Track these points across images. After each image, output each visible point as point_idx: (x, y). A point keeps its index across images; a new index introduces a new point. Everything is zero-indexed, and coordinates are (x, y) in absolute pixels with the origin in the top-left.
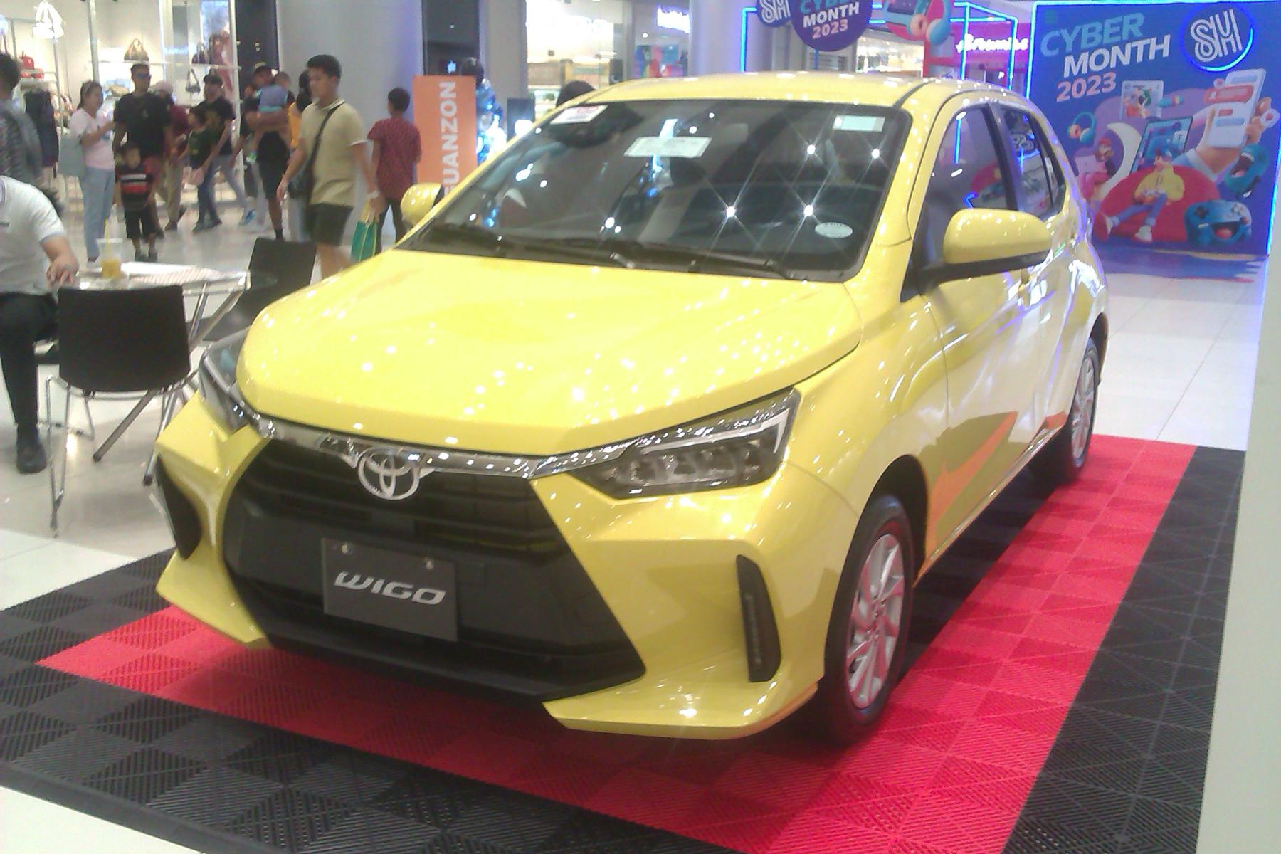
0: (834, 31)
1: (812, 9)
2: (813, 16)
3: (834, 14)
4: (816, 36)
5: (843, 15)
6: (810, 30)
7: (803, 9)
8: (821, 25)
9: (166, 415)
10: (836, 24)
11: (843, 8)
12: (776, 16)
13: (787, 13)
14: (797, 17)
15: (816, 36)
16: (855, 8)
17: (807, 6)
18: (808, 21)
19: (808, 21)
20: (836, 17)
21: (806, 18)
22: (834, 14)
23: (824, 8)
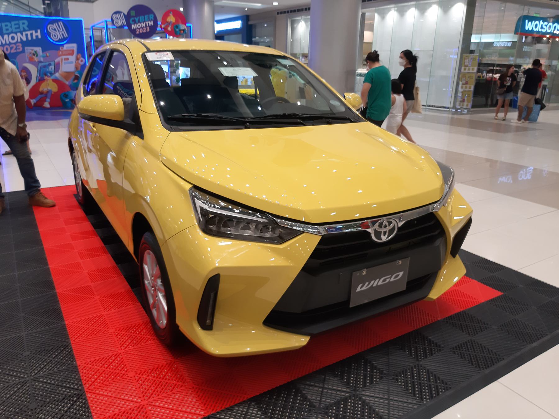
0: (144, 31)
1: (135, 22)
2: (136, 25)
3: (143, 25)
4: (137, 33)
6: (135, 30)
8: (139, 29)
9: (513, 119)
12: (120, 24)
13: (125, 23)
14: (129, 25)
15: (137, 33)
16: (151, 23)
18: (134, 27)
20: (144, 26)
21: (133, 26)
22: (143, 25)
23: (139, 22)
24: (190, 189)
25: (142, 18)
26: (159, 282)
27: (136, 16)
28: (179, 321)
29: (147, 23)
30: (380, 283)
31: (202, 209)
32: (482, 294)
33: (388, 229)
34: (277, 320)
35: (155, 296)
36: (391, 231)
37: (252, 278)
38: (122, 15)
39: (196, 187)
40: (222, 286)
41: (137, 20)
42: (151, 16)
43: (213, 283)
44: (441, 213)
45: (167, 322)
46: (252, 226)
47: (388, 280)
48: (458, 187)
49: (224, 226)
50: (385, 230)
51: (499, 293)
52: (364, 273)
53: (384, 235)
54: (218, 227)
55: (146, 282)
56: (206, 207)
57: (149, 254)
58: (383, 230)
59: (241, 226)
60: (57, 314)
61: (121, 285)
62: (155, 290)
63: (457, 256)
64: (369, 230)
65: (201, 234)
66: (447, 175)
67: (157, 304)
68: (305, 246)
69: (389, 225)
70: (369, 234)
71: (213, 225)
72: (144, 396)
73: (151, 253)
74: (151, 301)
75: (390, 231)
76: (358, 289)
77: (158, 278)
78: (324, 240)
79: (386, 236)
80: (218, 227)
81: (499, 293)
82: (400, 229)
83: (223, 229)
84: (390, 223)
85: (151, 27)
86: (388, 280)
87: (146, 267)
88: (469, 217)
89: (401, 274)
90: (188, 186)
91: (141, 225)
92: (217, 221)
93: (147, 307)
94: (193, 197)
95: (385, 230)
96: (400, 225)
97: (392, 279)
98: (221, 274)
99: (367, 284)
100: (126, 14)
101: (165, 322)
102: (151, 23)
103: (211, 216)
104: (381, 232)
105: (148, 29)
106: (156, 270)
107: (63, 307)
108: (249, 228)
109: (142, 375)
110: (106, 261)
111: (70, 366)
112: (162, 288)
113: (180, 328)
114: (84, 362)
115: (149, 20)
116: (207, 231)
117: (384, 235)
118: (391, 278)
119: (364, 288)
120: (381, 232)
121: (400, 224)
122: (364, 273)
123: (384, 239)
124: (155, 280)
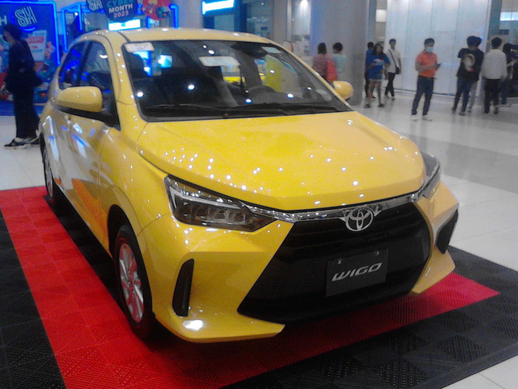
0: (123, 15)
1: (112, 5)
2: (113, 8)
3: (122, 8)
5: (126, 8)
6: (112, 14)
7: (108, 5)
8: (117, 13)
10: (124, 12)
11: (126, 6)
15: (115, 17)
16: (131, 6)
17: (110, 4)
18: (111, 10)
19: (111, 10)
20: (123, 9)
23: (117, 5)
24: (165, 179)
26: (135, 275)
28: (156, 309)
29: (126, 6)
30: (357, 273)
31: (177, 198)
32: (476, 293)
33: (362, 218)
34: (250, 307)
35: (131, 290)
36: (367, 221)
37: (225, 264)
39: (171, 176)
40: (196, 273)
41: (115, 3)
43: (187, 268)
44: (422, 204)
45: (143, 315)
46: (227, 214)
47: (365, 271)
48: (444, 179)
49: (199, 215)
50: (360, 219)
51: (494, 293)
52: (340, 262)
53: (360, 225)
54: (193, 215)
55: (122, 278)
56: (180, 195)
57: (125, 247)
58: (357, 219)
59: (215, 214)
60: (34, 312)
61: (96, 285)
62: (131, 283)
63: (447, 251)
64: (343, 219)
65: (175, 220)
66: (431, 166)
67: (133, 299)
68: (278, 232)
69: (364, 215)
70: (345, 223)
71: (189, 213)
72: (120, 383)
73: (127, 246)
74: (127, 296)
75: (364, 220)
76: (334, 279)
77: (135, 270)
78: (297, 228)
79: (361, 226)
80: (193, 215)
81: (494, 293)
82: (376, 219)
83: (197, 218)
84: (365, 212)
85: (130, 11)
86: (365, 271)
87: (122, 262)
88: (454, 211)
89: (380, 265)
90: (163, 176)
91: (117, 218)
92: (191, 211)
93: (122, 304)
94: (168, 186)
95: (360, 219)
96: (375, 215)
97: (370, 270)
98: (195, 260)
99: (343, 273)
101: (141, 315)
102: (131, 6)
103: (185, 204)
104: (356, 221)
105: (127, 12)
106: (132, 263)
107: (38, 305)
108: (223, 217)
109: (119, 365)
110: (80, 262)
111: (48, 357)
112: (138, 280)
113: (157, 317)
114: (61, 353)
116: (181, 219)
117: (360, 225)
118: (368, 269)
119: (340, 278)
120: (356, 221)
121: (376, 213)
122: (340, 262)
123: (359, 228)
124: (131, 274)
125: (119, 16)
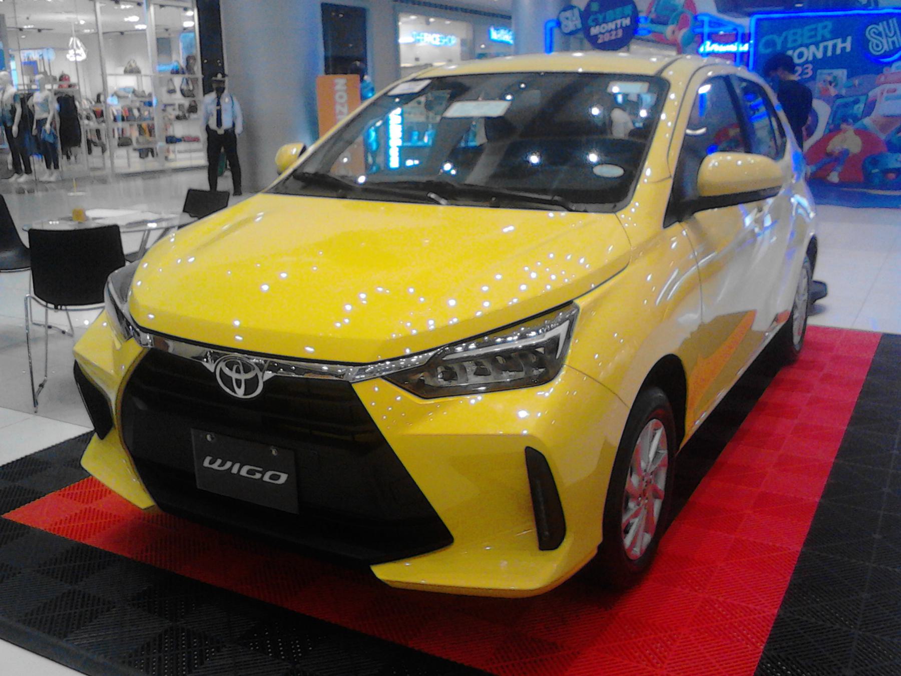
0: (613, 37)
2: (597, 27)
3: (612, 26)
4: (600, 41)
8: (603, 34)
11: (619, 22)
13: (579, 26)
14: (586, 29)
15: (600, 41)
16: (627, 22)
18: (594, 31)
19: (594, 31)
23: (605, 21)
25: (610, 14)
27: (600, 12)
38: (576, 12)
41: (600, 17)
42: (628, 10)
85: (625, 29)
100: (582, 7)
102: (627, 22)
105: (620, 33)
115: (624, 17)
125: (607, 39)
